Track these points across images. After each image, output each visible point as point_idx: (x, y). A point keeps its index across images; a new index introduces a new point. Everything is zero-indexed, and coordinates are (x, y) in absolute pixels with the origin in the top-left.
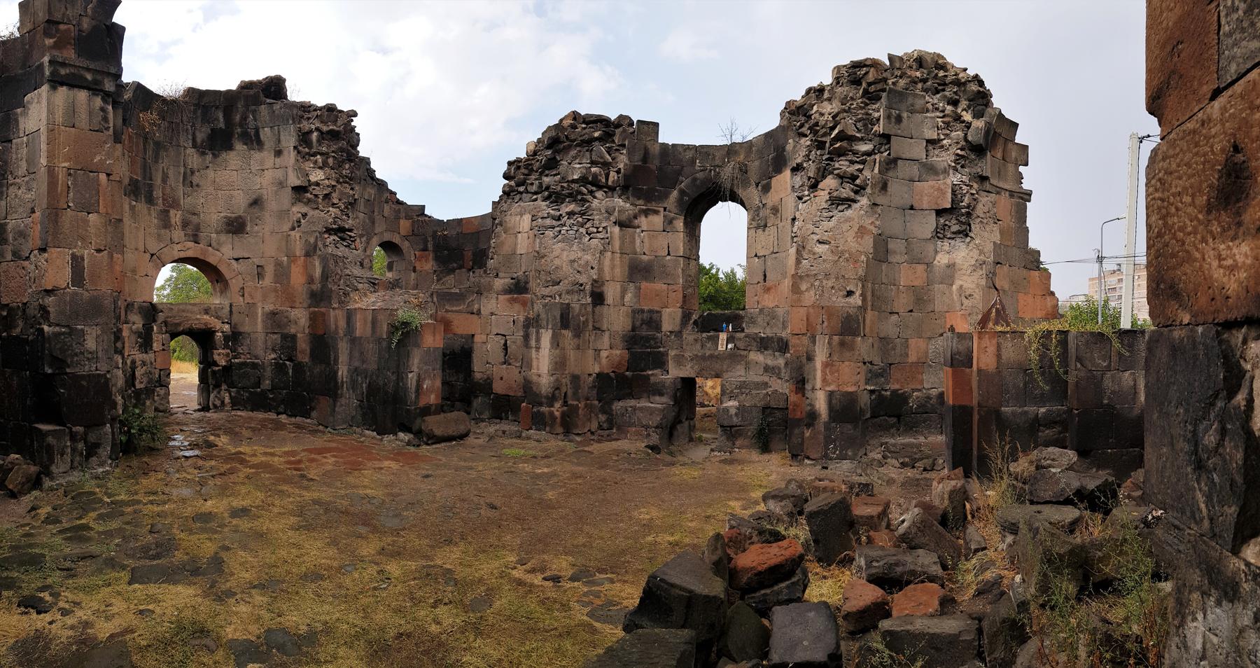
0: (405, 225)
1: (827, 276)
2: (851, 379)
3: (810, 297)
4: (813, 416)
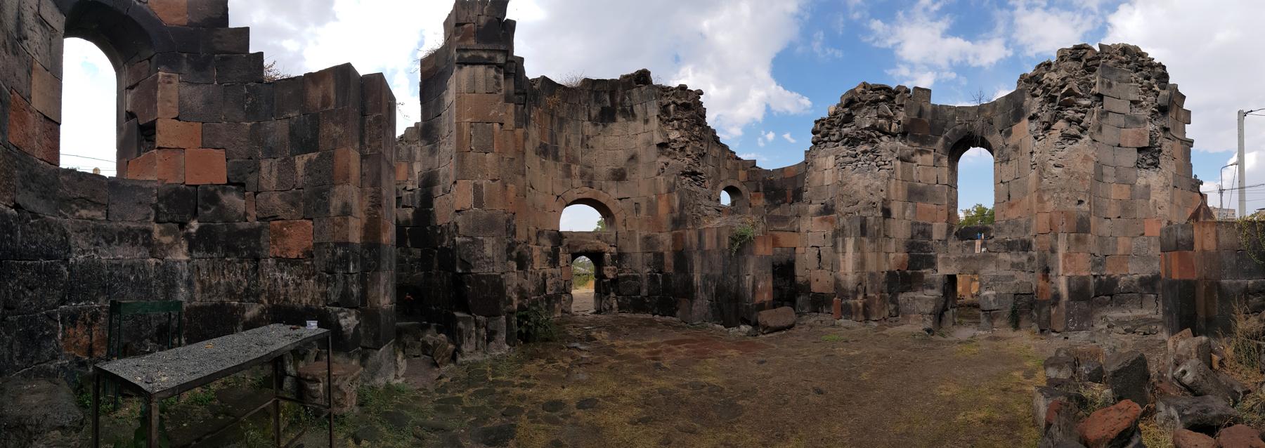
0: (742, 175)
1: (1063, 190)
2: (1083, 268)
3: (1050, 206)
4: (1057, 297)
